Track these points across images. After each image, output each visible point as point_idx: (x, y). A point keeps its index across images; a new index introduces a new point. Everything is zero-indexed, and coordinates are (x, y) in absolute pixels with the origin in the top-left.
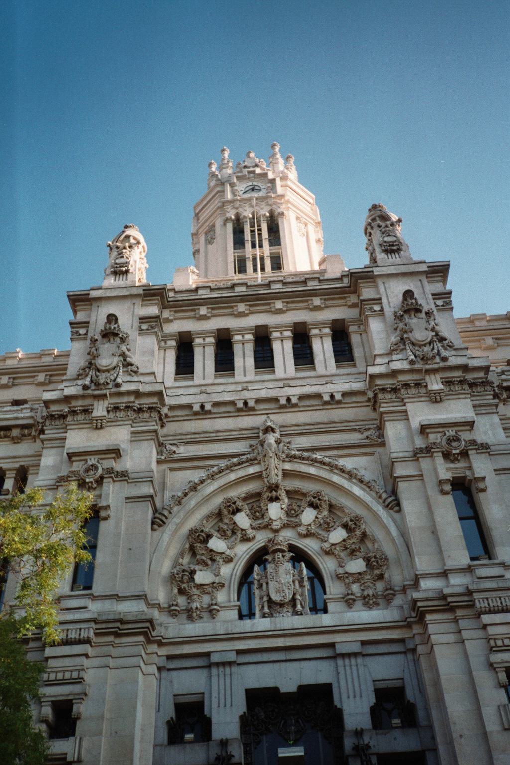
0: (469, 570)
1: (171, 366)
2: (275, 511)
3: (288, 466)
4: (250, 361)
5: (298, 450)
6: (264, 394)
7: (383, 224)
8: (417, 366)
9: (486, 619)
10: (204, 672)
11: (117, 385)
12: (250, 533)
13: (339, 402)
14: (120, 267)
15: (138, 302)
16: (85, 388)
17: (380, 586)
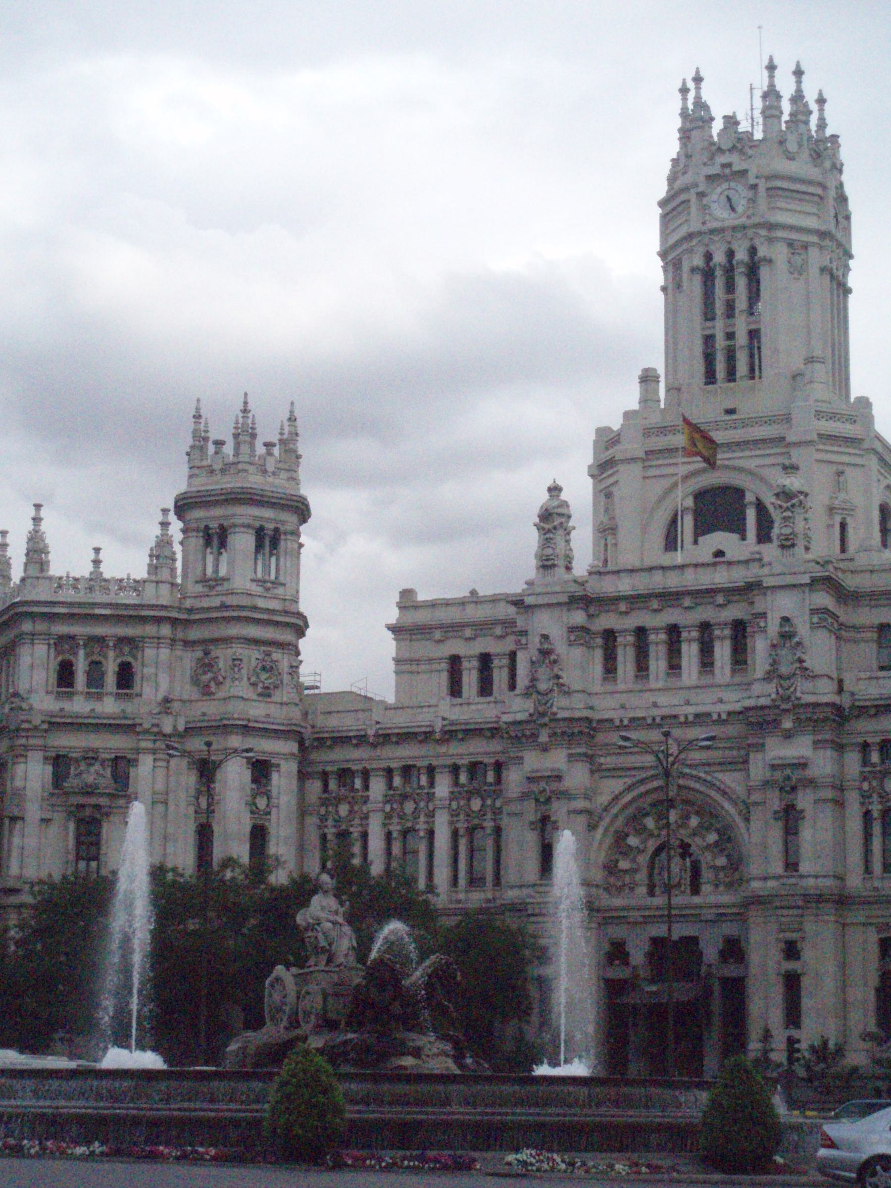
0: (781, 877)
1: (598, 669)
2: (673, 816)
3: (681, 782)
4: (663, 664)
5: (690, 766)
6: (666, 712)
7: (785, 505)
8: (777, 703)
9: (780, 912)
10: (626, 926)
11: (555, 714)
12: (656, 832)
13: (724, 720)
14: (548, 560)
15: (565, 609)
16: (531, 715)
17: (736, 876)
